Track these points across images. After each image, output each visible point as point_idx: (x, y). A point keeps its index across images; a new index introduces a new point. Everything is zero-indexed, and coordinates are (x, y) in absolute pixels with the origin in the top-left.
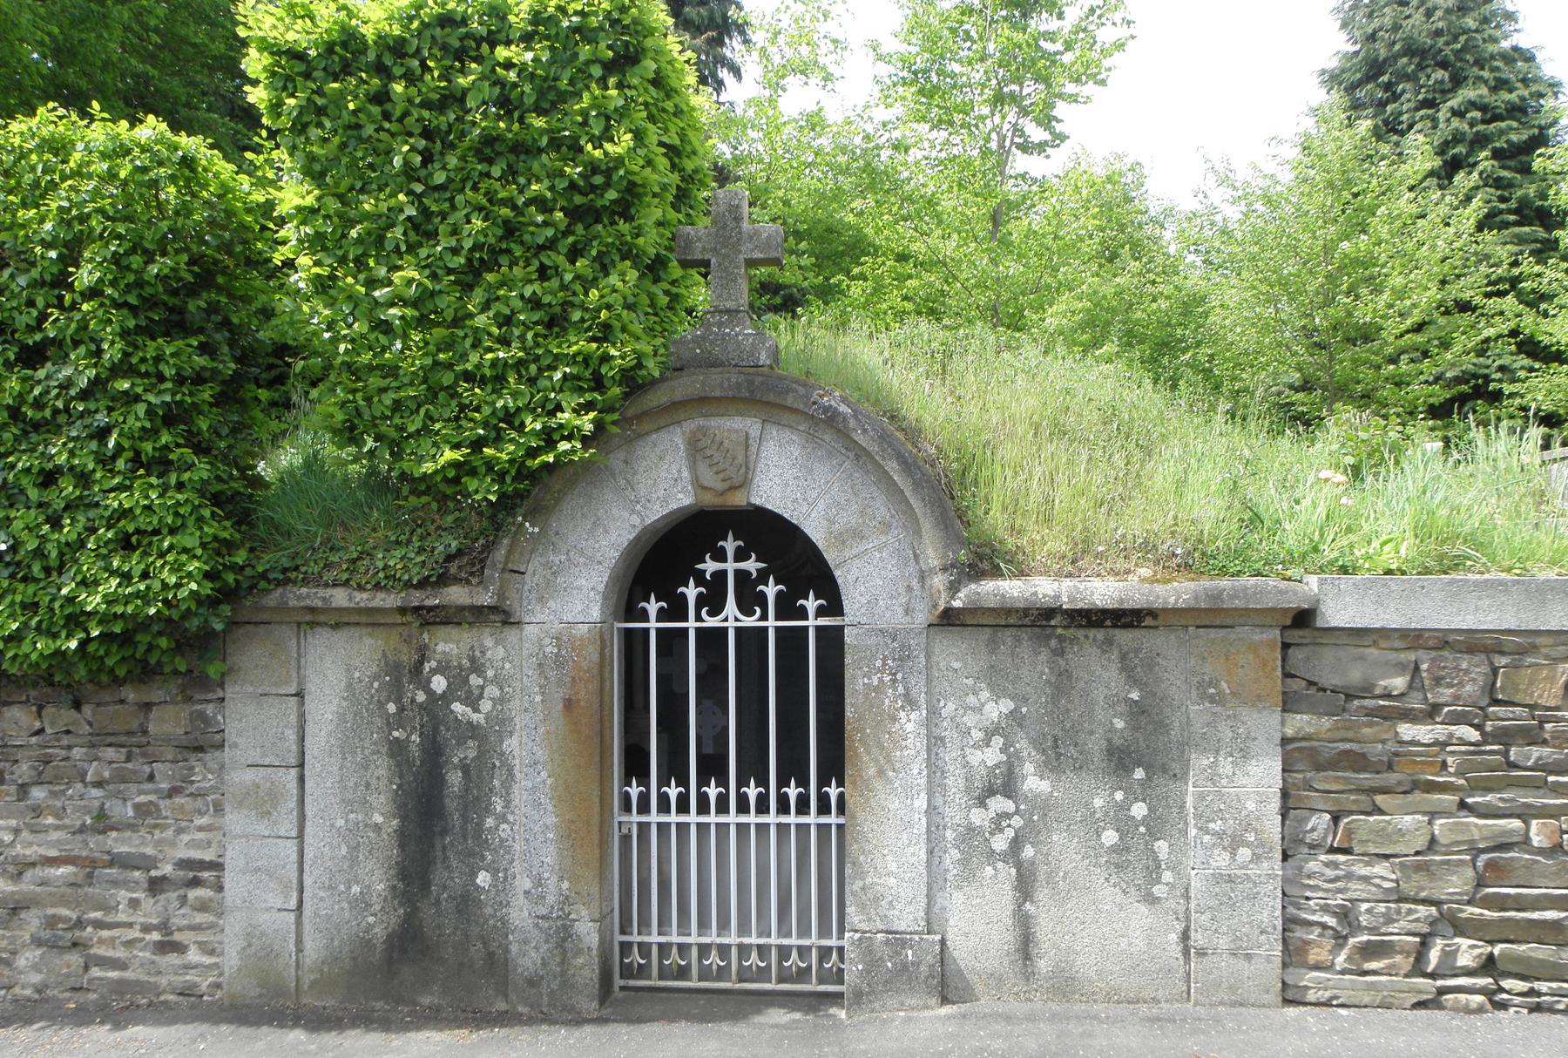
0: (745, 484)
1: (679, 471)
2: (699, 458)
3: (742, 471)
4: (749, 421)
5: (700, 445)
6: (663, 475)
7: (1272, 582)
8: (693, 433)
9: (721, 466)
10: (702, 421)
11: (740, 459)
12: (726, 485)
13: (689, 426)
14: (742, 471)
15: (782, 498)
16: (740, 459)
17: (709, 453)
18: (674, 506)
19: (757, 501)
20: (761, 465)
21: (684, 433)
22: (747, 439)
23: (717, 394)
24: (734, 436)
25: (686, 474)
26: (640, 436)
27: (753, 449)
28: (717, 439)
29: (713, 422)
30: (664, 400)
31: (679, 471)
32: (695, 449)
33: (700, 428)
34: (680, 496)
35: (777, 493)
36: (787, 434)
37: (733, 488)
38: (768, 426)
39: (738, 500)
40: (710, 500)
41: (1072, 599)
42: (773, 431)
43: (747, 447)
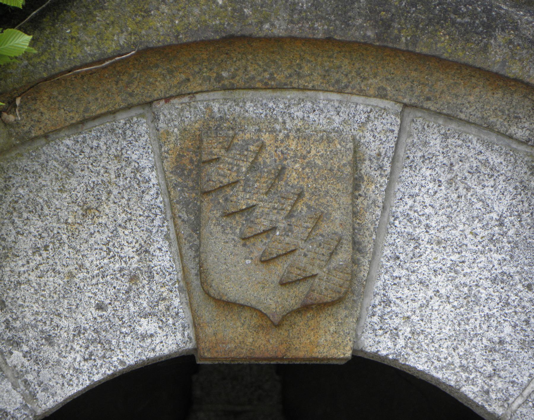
0: (346, 296)
1: (144, 251)
2: (211, 212)
3: (343, 256)
4: (361, 106)
5: (216, 174)
6: (93, 260)
7: (343, 38)
8: (196, 140)
9: (278, 243)
10: (217, 104)
11: (337, 221)
12: (293, 297)
13: (179, 116)
14: (343, 256)
15: (459, 338)
16: (337, 221)
17: (242, 199)
18: (128, 355)
19: (380, 345)
20: (394, 241)
21: (160, 138)
22: (356, 161)
23: (279, 27)
24: (316, 152)
25: (164, 259)
26: (27, 140)
27: (374, 190)
28: (267, 158)
29: (253, 107)
30: (117, 40)
31: (144, 251)
32: (197, 185)
33: (213, 126)
34: (147, 326)
35: (441, 320)
36: (472, 148)
37: (310, 307)
38: (418, 121)
39: (326, 342)
40: (237, 340)
41: (78, 128)
42: (434, 138)
43: (357, 182)
